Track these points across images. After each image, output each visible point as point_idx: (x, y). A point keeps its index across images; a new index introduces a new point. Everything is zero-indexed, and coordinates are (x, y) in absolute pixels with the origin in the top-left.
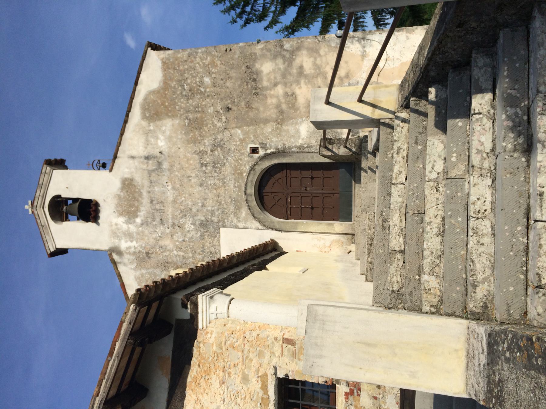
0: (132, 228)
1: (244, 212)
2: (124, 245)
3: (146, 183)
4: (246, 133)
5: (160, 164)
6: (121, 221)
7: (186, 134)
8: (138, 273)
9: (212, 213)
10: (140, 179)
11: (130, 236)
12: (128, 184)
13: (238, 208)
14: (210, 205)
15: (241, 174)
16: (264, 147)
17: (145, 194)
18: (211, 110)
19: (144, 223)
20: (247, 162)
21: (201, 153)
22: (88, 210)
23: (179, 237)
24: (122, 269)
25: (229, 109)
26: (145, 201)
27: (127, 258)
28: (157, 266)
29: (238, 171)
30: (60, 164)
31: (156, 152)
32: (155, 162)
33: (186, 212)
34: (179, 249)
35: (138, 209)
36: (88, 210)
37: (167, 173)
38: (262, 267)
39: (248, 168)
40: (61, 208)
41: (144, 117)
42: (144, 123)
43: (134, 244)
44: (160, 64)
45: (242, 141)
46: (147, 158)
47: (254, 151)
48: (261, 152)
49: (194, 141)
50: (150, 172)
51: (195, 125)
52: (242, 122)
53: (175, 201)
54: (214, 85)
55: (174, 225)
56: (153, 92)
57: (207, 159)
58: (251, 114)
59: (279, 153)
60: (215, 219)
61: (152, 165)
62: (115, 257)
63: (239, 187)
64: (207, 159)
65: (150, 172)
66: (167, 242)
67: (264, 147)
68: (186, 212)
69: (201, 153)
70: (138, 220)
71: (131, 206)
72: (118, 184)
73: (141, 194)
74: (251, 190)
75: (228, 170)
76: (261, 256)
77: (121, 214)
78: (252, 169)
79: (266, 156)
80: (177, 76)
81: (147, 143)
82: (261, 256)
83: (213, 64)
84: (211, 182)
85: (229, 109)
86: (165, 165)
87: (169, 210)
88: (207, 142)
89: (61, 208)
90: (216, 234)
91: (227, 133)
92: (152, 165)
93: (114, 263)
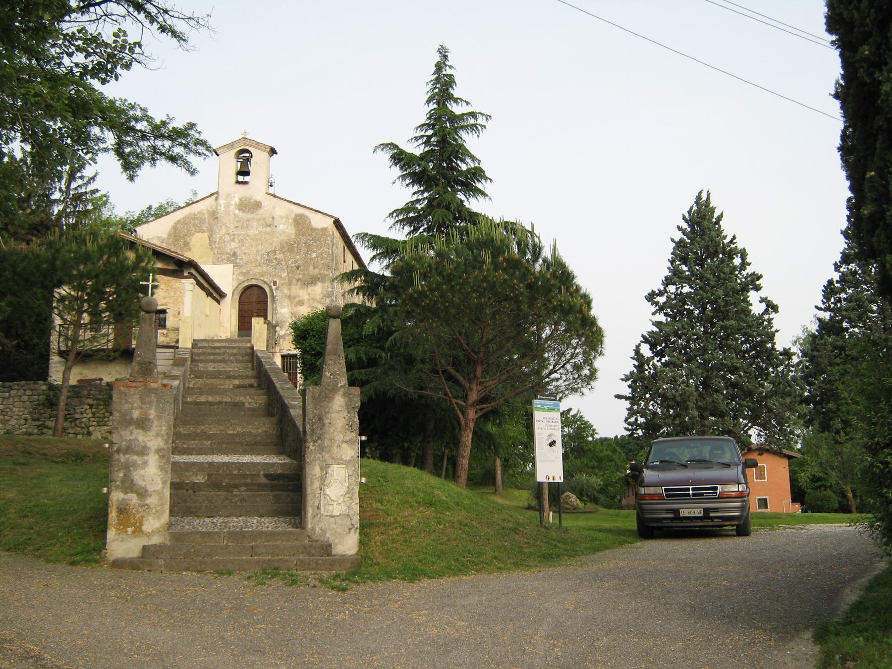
3: (258, 217)
4: (284, 279)
5: (270, 226)
7: (286, 243)
9: (241, 259)
11: (228, 206)
12: (258, 205)
13: (244, 274)
15: (262, 276)
16: (277, 289)
17: (253, 216)
18: (298, 257)
19: (235, 216)
23: (227, 238)
25: (298, 268)
28: (210, 224)
29: (261, 275)
34: (220, 238)
35: (244, 211)
38: (209, 294)
39: (266, 280)
41: (296, 216)
42: (293, 216)
43: (223, 209)
44: (325, 226)
45: (280, 276)
47: (275, 283)
48: (274, 287)
49: (282, 247)
51: (289, 247)
53: (248, 235)
54: (311, 259)
58: (294, 281)
59: (273, 297)
60: (238, 261)
63: (255, 275)
67: (277, 289)
69: (274, 252)
70: (237, 212)
71: (245, 207)
73: (252, 213)
74: (254, 282)
75: (265, 268)
76: (214, 292)
77: (240, 200)
78: (265, 282)
80: (318, 237)
81: (282, 218)
82: (214, 292)
83: (323, 258)
84: (259, 258)
86: (268, 229)
88: (279, 256)
90: (229, 261)
91: (285, 267)
92: (269, 220)
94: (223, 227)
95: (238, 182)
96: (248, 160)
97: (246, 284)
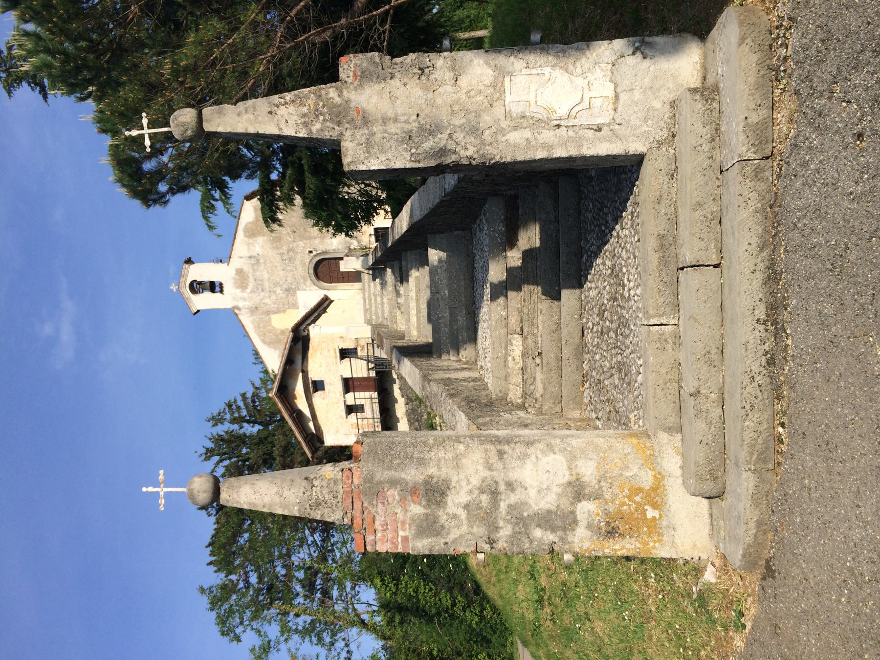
0: (245, 295)
1: (309, 282)
2: (241, 304)
3: (251, 271)
4: (305, 244)
5: (258, 260)
6: (238, 292)
8: (252, 318)
9: (292, 284)
10: (247, 268)
12: (240, 272)
13: (305, 280)
14: (290, 280)
16: (316, 250)
17: (251, 276)
19: (252, 292)
20: (307, 258)
21: (282, 254)
22: (213, 287)
23: (274, 297)
24: (241, 317)
25: (294, 232)
26: (251, 279)
27: (243, 311)
28: (263, 314)
29: (303, 264)
30: (189, 261)
31: (255, 254)
32: (255, 260)
33: (276, 284)
34: (275, 303)
35: (247, 285)
36: (213, 287)
37: (263, 265)
38: (324, 311)
40: (196, 287)
41: (246, 236)
42: (246, 239)
43: (247, 303)
45: (304, 247)
46: (250, 257)
47: (311, 252)
48: (314, 253)
49: (277, 248)
50: (253, 265)
52: (302, 238)
53: (269, 279)
55: (270, 292)
56: (250, 223)
57: (285, 257)
58: (307, 234)
59: (323, 253)
61: (253, 261)
62: (236, 311)
64: (285, 257)
65: (253, 265)
66: (267, 301)
67: (316, 250)
68: (276, 284)
69: (282, 254)
70: (248, 290)
72: (234, 272)
73: (248, 277)
74: (312, 271)
75: (297, 262)
76: (323, 306)
77: (237, 288)
78: (311, 261)
79: (317, 255)
81: (249, 250)
82: (323, 306)
84: (289, 268)
85: (294, 232)
86: (261, 261)
87: (267, 285)
88: (285, 248)
89: (196, 287)
90: (294, 294)
91: (295, 244)
92: (253, 261)
93: (236, 315)
94: (264, 301)
95: (221, 291)
96: (200, 283)
97: (314, 278)
